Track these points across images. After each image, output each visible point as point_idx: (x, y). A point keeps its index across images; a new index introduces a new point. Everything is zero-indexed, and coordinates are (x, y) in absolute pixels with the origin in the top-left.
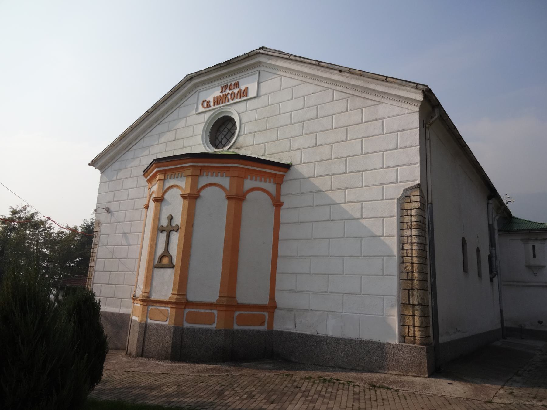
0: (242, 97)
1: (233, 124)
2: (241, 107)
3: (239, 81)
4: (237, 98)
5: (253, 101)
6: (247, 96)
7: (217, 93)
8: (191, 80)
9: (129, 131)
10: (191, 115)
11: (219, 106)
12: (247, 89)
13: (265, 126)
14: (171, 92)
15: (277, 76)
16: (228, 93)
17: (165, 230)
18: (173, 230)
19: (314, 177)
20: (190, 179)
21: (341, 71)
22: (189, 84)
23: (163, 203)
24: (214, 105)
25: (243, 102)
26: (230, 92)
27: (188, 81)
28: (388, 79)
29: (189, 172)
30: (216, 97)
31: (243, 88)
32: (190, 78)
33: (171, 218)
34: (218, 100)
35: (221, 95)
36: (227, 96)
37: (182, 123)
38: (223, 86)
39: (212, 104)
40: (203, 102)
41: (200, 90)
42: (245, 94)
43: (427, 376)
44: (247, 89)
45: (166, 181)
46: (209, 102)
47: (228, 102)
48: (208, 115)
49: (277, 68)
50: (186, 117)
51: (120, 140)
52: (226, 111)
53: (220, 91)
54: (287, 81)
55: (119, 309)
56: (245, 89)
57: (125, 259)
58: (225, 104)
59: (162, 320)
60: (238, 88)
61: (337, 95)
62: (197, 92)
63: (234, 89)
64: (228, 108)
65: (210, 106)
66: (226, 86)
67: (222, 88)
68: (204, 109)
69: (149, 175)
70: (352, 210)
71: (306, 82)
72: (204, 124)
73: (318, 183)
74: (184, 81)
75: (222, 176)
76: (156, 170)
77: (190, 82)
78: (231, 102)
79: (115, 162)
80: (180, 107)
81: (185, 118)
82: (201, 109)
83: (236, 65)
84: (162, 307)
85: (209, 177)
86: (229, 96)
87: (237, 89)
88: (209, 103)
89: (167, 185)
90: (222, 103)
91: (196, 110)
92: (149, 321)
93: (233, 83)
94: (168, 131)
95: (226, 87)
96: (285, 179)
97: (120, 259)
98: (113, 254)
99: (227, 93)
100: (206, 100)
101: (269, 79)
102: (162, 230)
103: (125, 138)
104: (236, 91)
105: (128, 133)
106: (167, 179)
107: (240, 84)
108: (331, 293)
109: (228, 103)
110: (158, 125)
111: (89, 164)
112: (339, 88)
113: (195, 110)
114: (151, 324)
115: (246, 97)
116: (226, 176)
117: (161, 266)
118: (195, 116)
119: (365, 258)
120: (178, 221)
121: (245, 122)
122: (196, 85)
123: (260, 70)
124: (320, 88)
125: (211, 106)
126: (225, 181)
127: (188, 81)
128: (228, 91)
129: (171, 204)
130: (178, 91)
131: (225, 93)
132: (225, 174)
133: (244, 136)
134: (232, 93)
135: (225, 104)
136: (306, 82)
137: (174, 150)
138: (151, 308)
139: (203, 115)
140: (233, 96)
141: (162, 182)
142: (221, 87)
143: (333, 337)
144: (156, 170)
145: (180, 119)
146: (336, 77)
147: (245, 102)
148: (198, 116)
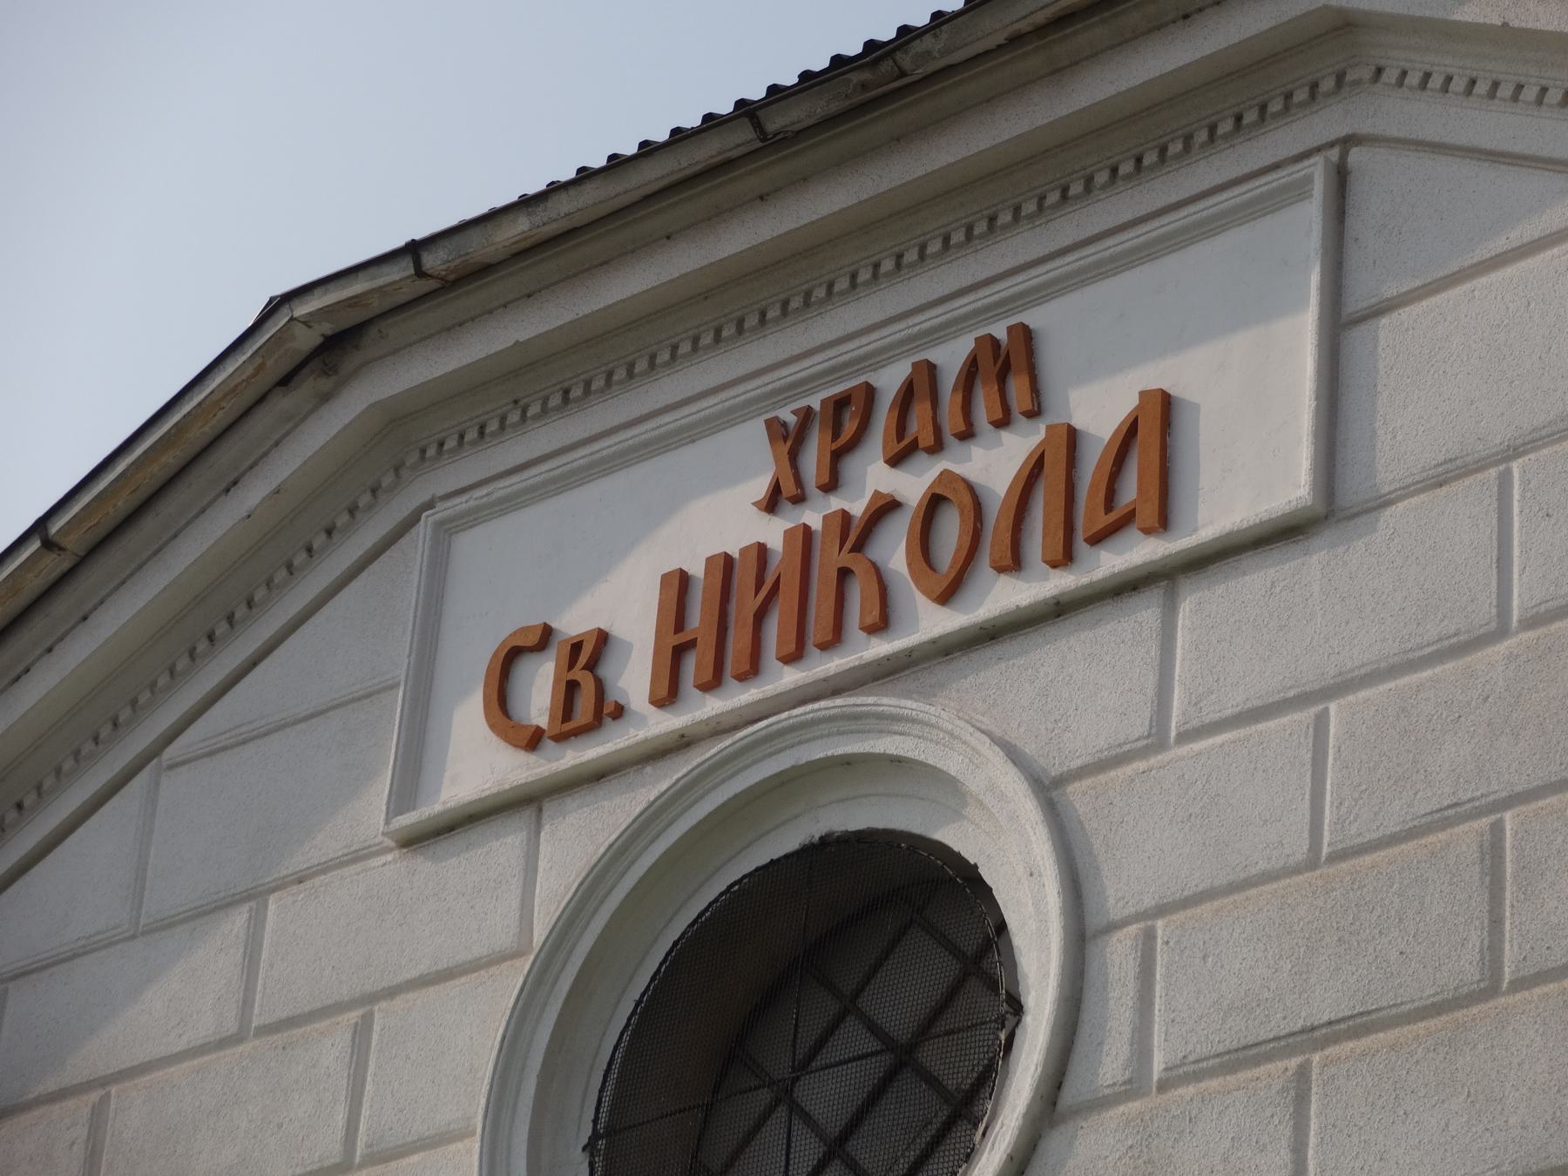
0: (1097, 539)
1: (954, 950)
3: (1033, 318)
4: (1013, 563)
6: (1163, 522)
8: (329, 370)
10: (325, 868)
11: (738, 697)
13: (1476, 938)
14: (48, 545)
16: (886, 507)
22: (296, 421)
24: (667, 695)
25: (1108, 608)
26: (912, 485)
27: (286, 381)
30: (697, 570)
35: (775, 542)
36: (859, 547)
38: (806, 415)
40: (510, 658)
41: (460, 504)
42: (1129, 491)
47: (881, 624)
50: (256, 896)
52: (847, 762)
53: (760, 487)
56: (1130, 433)
60: (1034, 413)
62: (428, 520)
65: (608, 712)
66: (840, 404)
67: (789, 440)
68: (531, 758)
72: (512, 979)
74: (229, 391)
77: (325, 398)
80: (170, 753)
81: (238, 920)
83: (990, 100)
87: (1005, 435)
88: (592, 666)
90: (793, 657)
91: (406, 790)
93: (951, 357)
100: (547, 633)
101: (1500, 244)
107: (1054, 360)
109: (880, 648)
115: (1147, 531)
118: (391, 867)
121: (1148, 902)
123: (1348, 142)
125: (619, 712)
127: (286, 381)
130: (149, 525)
131: (835, 503)
133: (1134, 1106)
134: (934, 503)
140: (950, 531)
142: (776, 430)
145: (166, 924)
147: (1144, 614)
148: (422, 866)
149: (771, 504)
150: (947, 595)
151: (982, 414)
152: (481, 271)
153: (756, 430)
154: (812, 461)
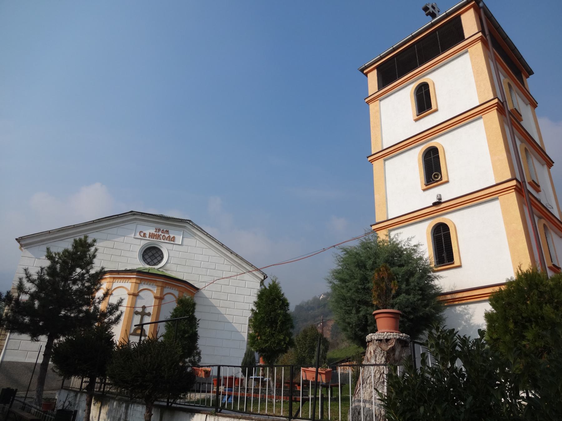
2: (170, 246)
3: (169, 230)
4: (167, 240)
5: (177, 246)
7: (153, 231)
12: (174, 237)
15: (194, 238)
16: (161, 235)
17: (140, 314)
18: (147, 315)
19: (211, 298)
20: (160, 288)
21: (231, 253)
23: (138, 297)
24: (149, 237)
26: (163, 234)
28: (253, 266)
29: (160, 284)
30: (151, 233)
31: (172, 236)
32: (132, 213)
33: (144, 308)
34: (151, 236)
37: (121, 239)
39: (148, 236)
42: (173, 240)
44: (174, 237)
45: (140, 285)
46: (145, 234)
47: (160, 239)
48: (143, 243)
49: (196, 234)
50: (125, 236)
53: (155, 231)
54: (199, 243)
56: (173, 237)
58: (158, 240)
60: (168, 234)
61: (226, 262)
63: (165, 233)
64: (160, 244)
65: (145, 237)
66: (159, 229)
67: (156, 229)
70: (229, 318)
73: (213, 302)
75: (175, 290)
76: (135, 276)
78: (163, 241)
80: (120, 227)
81: (124, 237)
82: (138, 236)
85: (169, 289)
86: (161, 237)
89: (141, 288)
91: (134, 236)
93: (165, 230)
94: (106, 240)
95: (159, 230)
96: (195, 295)
99: (160, 234)
102: (137, 313)
104: (167, 235)
106: (141, 284)
108: (215, 355)
109: (160, 241)
110: (96, 232)
111: (16, 239)
112: (228, 259)
113: (133, 235)
116: (177, 290)
117: (136, 334)
120: (150, 310)
122: (136, 219)
124: (218, 256)
126: (176, 293)
128: (160, 233)
129: (144, 299)
132: (176, 289)
134: (164, 235)
135: (158, 240)
137: (112, 255)
139: (139, 240)
141: (138, 285)
146: (229, 254)
147: (172, 245)
148: (135, 239)
149: (155, 232)
150: (164, 240)
151: (166, 233)
153: (155, 228)
154: (157, 231)
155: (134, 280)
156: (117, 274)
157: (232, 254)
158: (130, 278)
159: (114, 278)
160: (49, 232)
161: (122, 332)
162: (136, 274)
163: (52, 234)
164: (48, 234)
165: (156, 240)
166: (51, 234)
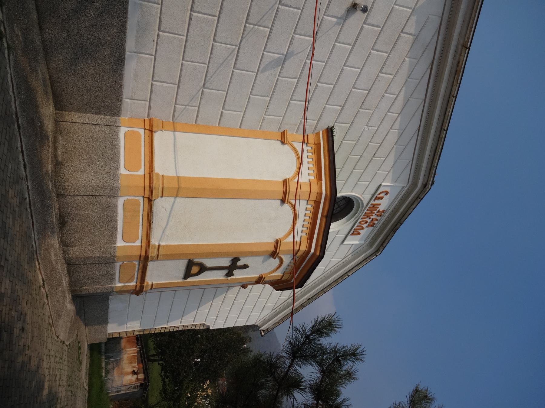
9: (454, 87)
21: (309, 299)
22: (423, 181)
43: (88, 343)
51: (458, 63)
52: (355, 215)
55: (134, 49)
57: (233, 65)
59: (120, 278)
69: (322, 216)
71: (322, 274)
76: (313, 251)
79: (440, 25)
80: (411, 162)
84: (138, 275)
92: (118, 265)
97: (237, 47)
98: (254, 25)
103: (454, 72)
105: (455, 83)
110: (419, 127)
114: (114, 267)
119: (169, 314)
122: (414, 184)
136: (322, 274)
138: (136, 265)
143: (108, 308)
144: (313, 251)
150: (360, 223)
152: (417, 199)
155: (304, 248)
156: (325, 214)
157: (306, 300)
158: (311, 238)
159: (317, 203)
160: (468, 46)
161: (198, 245)
162: (318, 254)
163: (456, 51)
164: (461, 42)
165: (365, 212)
166: (460, 47)
